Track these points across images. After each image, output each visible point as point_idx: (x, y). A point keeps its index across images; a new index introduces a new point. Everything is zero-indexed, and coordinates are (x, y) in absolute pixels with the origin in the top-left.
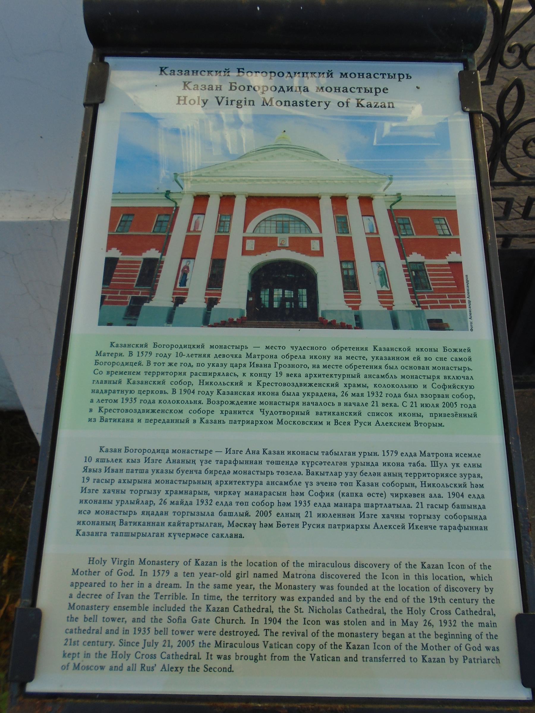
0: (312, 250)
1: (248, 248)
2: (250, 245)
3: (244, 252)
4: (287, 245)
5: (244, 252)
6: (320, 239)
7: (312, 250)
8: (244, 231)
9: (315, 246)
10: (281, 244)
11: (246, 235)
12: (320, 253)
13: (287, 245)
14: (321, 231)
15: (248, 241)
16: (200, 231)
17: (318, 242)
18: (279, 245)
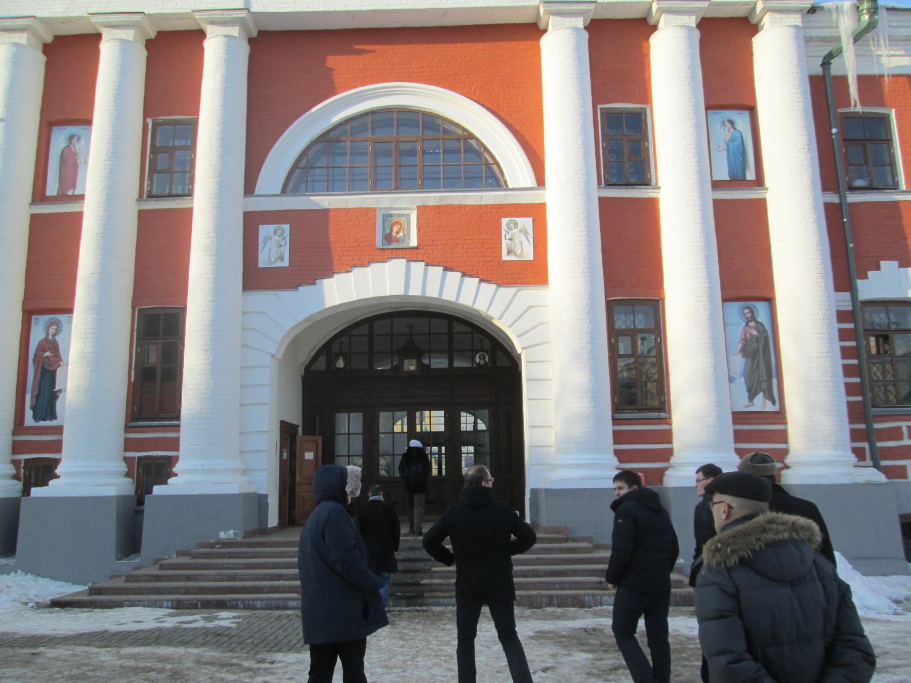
0: (505, 257)
1: (264, 261)
2: (275, 249)
3: (255, 278)
4: (414, 242)
5: (255, 278)
6: (537, 212)
7: (505, 257)
8: (249, 188)
9: (516, 241)
10: (388, 238)
11: (256, 205)
12: (533, 273)
13: (414, 242)
14: (541, 182)
15: (265, 230)
16: (81, 197)
17: (526, 223)
18: (379, 243)
